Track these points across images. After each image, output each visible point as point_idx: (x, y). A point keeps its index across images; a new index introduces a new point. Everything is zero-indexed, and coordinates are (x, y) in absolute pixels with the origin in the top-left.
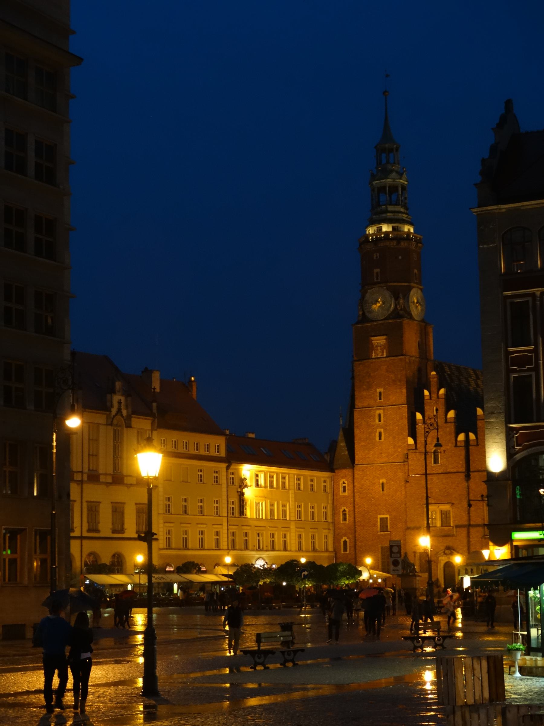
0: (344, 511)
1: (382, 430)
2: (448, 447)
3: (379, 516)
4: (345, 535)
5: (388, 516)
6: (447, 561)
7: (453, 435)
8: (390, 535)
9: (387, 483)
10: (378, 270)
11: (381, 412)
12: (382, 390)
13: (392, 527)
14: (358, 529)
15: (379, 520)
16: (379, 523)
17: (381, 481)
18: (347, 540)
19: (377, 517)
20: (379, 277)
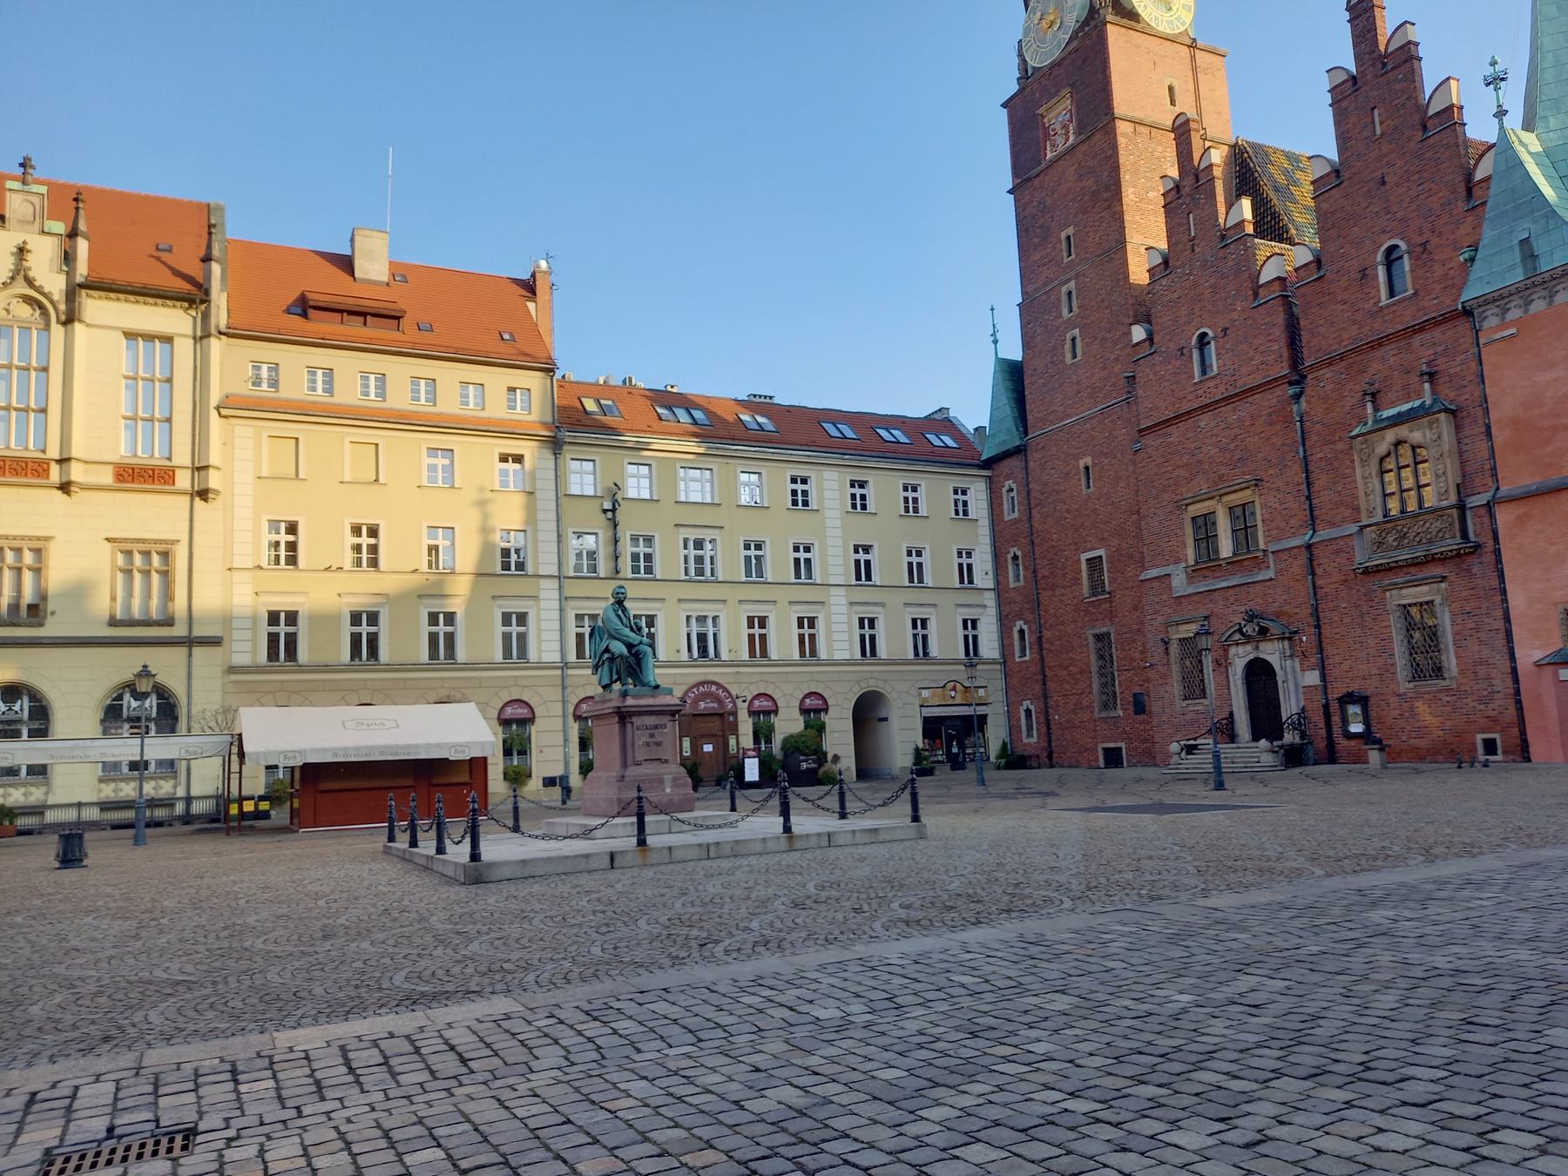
0: (1015, 558)
1: (1077, 331)
2: (1235, 315)
3: (1084, 557)
4: (1019, 616)
5: (1101, 552)
6: (1252, 657)
8: (1110, 600)
9: (1094, 465)
11: (1072, 284)
12: (1070, 231)
13: (1113, 580)
14: (1044, 595)
15: (1084, 566)
16: (1084, 574)
17: (1082, 464)
18: (1025, 627)
19: (1079, 560)
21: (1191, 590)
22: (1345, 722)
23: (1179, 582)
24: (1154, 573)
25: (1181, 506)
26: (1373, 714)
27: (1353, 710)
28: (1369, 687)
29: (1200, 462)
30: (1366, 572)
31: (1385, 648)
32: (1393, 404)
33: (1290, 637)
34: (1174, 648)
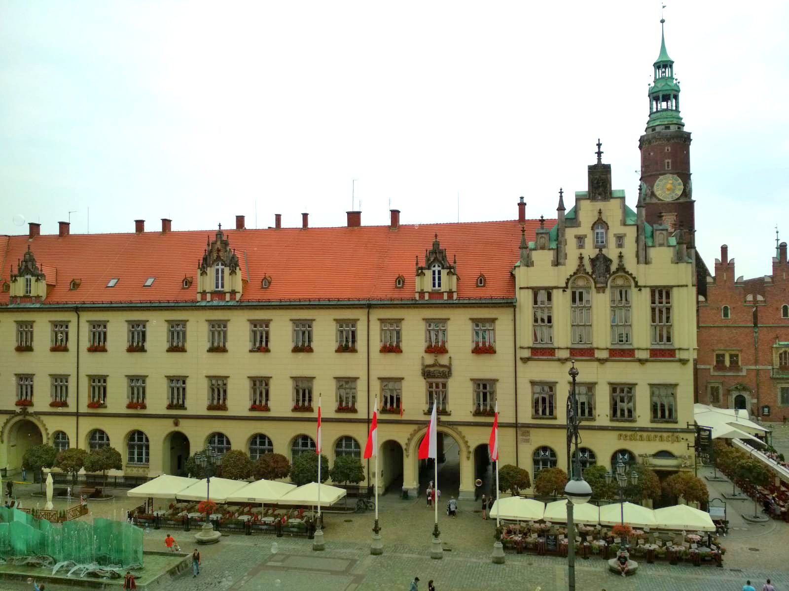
7: (743, 296)
10: (670, 161)
20: (670, 167)
21: (716, 374)
22: (763, 410)
23: (712, 370)
24: (702, 367)
25: (713, 350)
26: (771, 411)
27: (766, 410)
28: (771, 404)
29: (721, 340)
30: (772, 378)
31: (776, 397)
32: (782, 341)
33: (751, 392)
34: (709, 389)
